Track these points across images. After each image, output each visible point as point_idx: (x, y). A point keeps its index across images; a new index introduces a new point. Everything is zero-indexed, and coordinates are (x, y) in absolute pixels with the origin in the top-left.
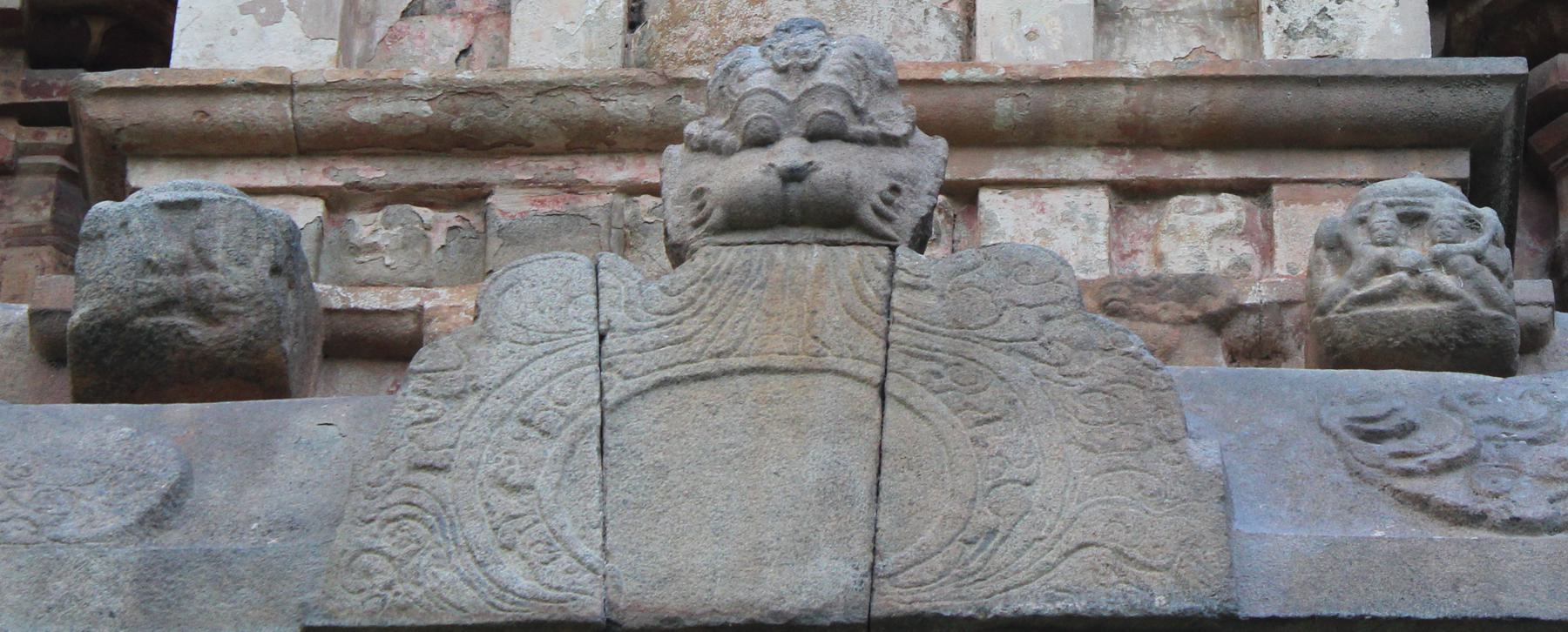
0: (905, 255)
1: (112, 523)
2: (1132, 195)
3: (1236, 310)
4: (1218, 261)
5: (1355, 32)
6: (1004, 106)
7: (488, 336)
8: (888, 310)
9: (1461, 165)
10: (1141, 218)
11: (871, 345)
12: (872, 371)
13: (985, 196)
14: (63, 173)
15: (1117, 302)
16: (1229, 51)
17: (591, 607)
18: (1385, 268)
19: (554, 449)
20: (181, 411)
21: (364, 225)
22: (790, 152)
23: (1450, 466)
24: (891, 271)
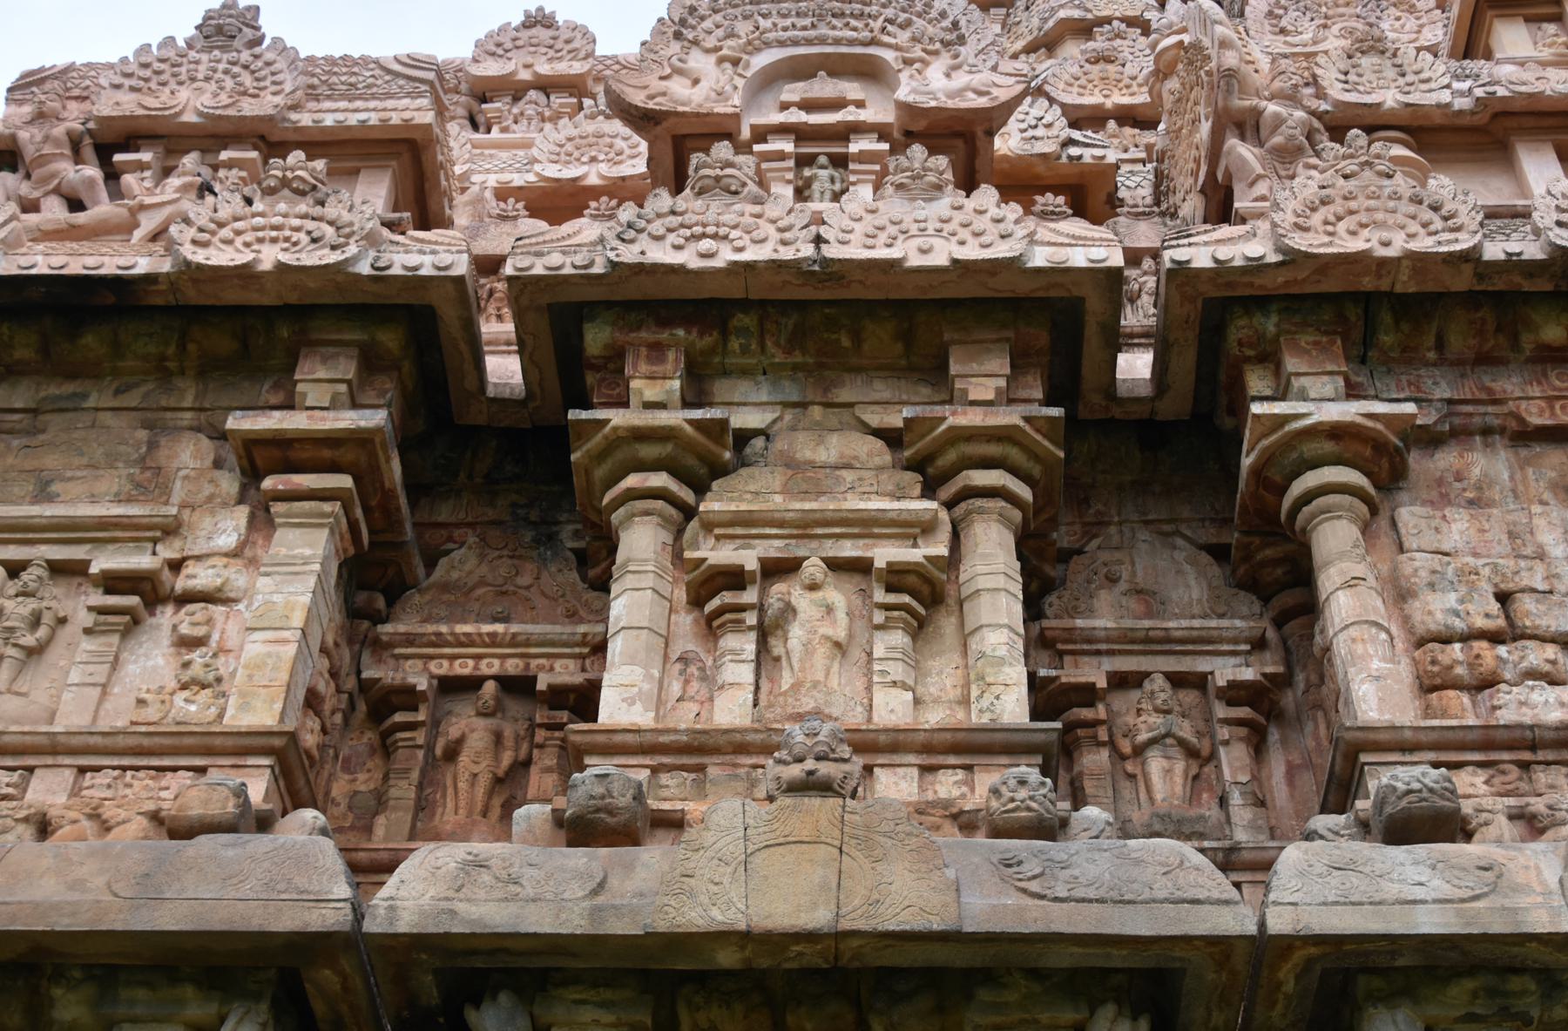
0: (848, 800)
1: (581, 894)
2: (926, 769)
3: (962, 812)
4: (956, 793)
5: (1003, 711)
6: (882, 738)
7: (707, 829)
8: (842, 822)
9: (1039, 760)
10: (929, 777)
11: (837, 833)
12: (837, 843)
13: (876, 770)
14: (561, 747)
15: (921, 810)
16: (959, 717)
17: (742, 926)
18: (1012, 800)
19: (729, 870)
20: (604, 851)
21: (664, 778)
22: (810, 764)
23: (1034, 877)
24: (844, 807)
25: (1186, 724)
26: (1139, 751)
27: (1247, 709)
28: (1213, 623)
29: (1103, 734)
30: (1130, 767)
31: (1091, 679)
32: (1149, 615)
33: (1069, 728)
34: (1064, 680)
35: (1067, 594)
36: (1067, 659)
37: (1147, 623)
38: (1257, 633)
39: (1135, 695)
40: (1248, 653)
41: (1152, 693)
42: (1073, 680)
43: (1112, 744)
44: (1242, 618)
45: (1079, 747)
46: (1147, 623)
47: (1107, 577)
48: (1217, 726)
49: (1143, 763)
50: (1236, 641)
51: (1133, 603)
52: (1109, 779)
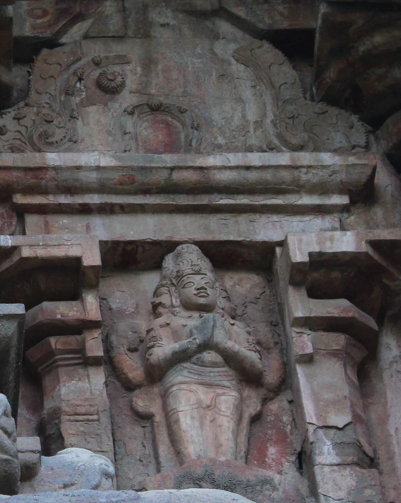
25: (239, 329)
26: (156, 375)
27: (344, 303)
28: (284, 158)
29: (94, 346)
30: (141, 403)
31: (74, 252)
32: (171, 147)
33: (35, 335)
34: (26, 253)
35: (30, 114)
36: (31, 220)
37: (169, 159)
38: (360, 176)
39: (149, 281)
40: (344, 209)
41: (180, 276)
42: (41, 253)
43: (108, 362)
44: (336, 151)
45: (53, 368)
46: (169, 159)
47: (99, 85)
48: (293, 332)
49: (165, 396)
50: (322, 189)
51: (146, 129)
52: (105, 420)
